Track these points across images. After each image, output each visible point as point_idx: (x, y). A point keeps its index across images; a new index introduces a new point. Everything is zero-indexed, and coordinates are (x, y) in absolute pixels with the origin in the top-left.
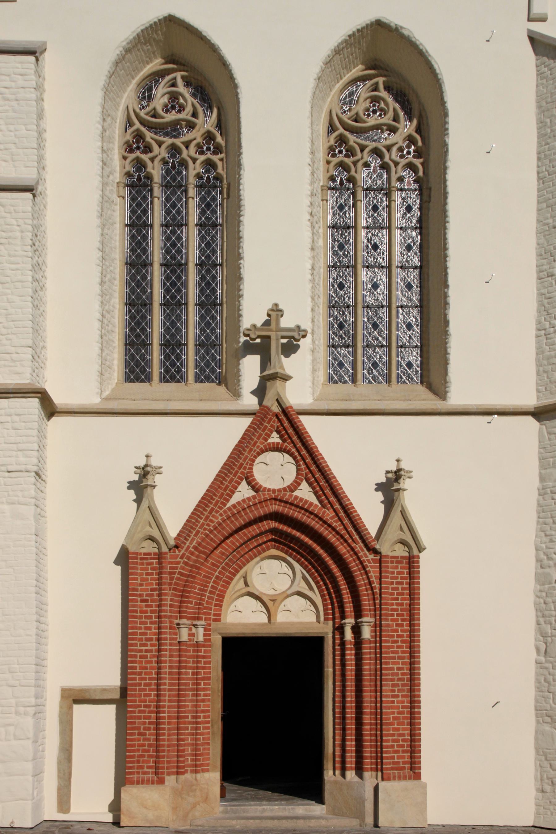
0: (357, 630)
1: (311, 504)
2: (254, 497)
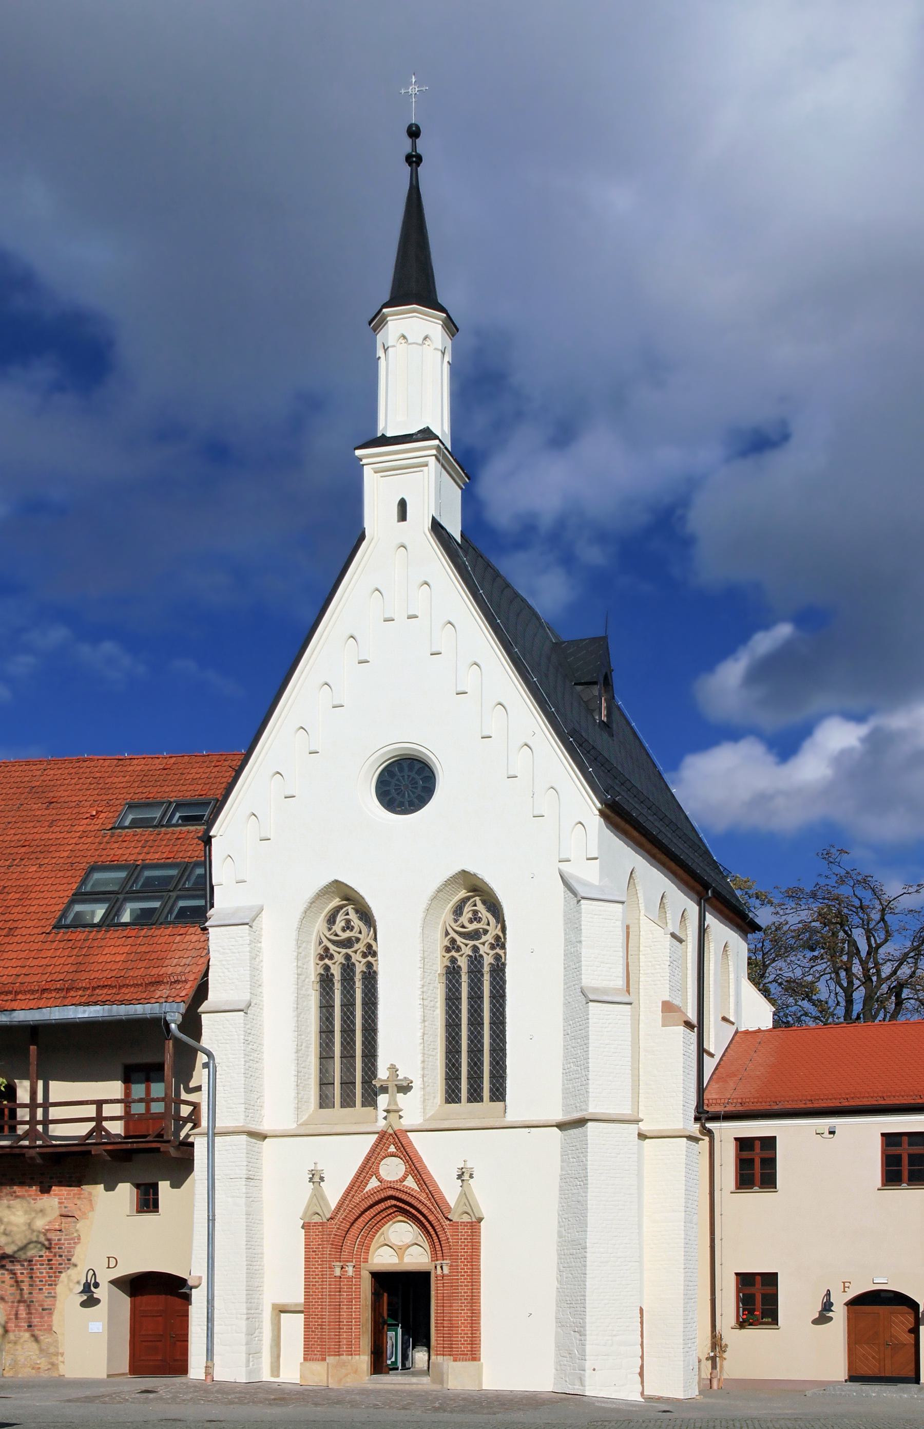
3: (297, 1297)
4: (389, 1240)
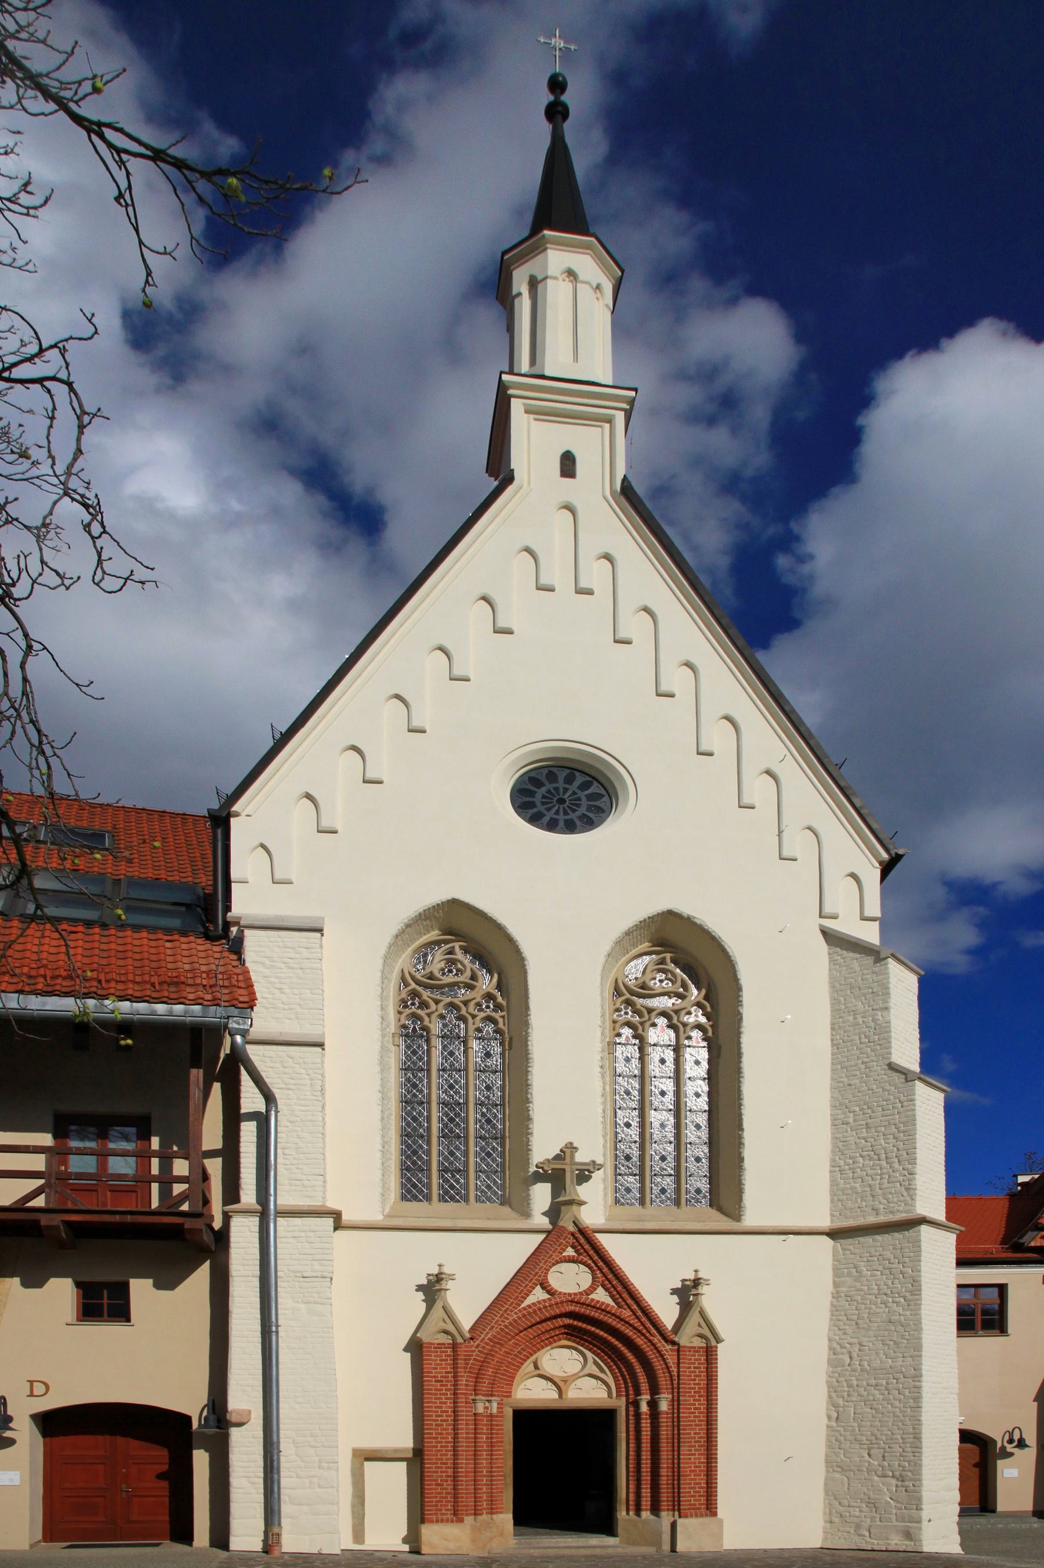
0: (653, 1404)
1: (608, 1305)
2: (549, 1299)
3: (406, 1441)
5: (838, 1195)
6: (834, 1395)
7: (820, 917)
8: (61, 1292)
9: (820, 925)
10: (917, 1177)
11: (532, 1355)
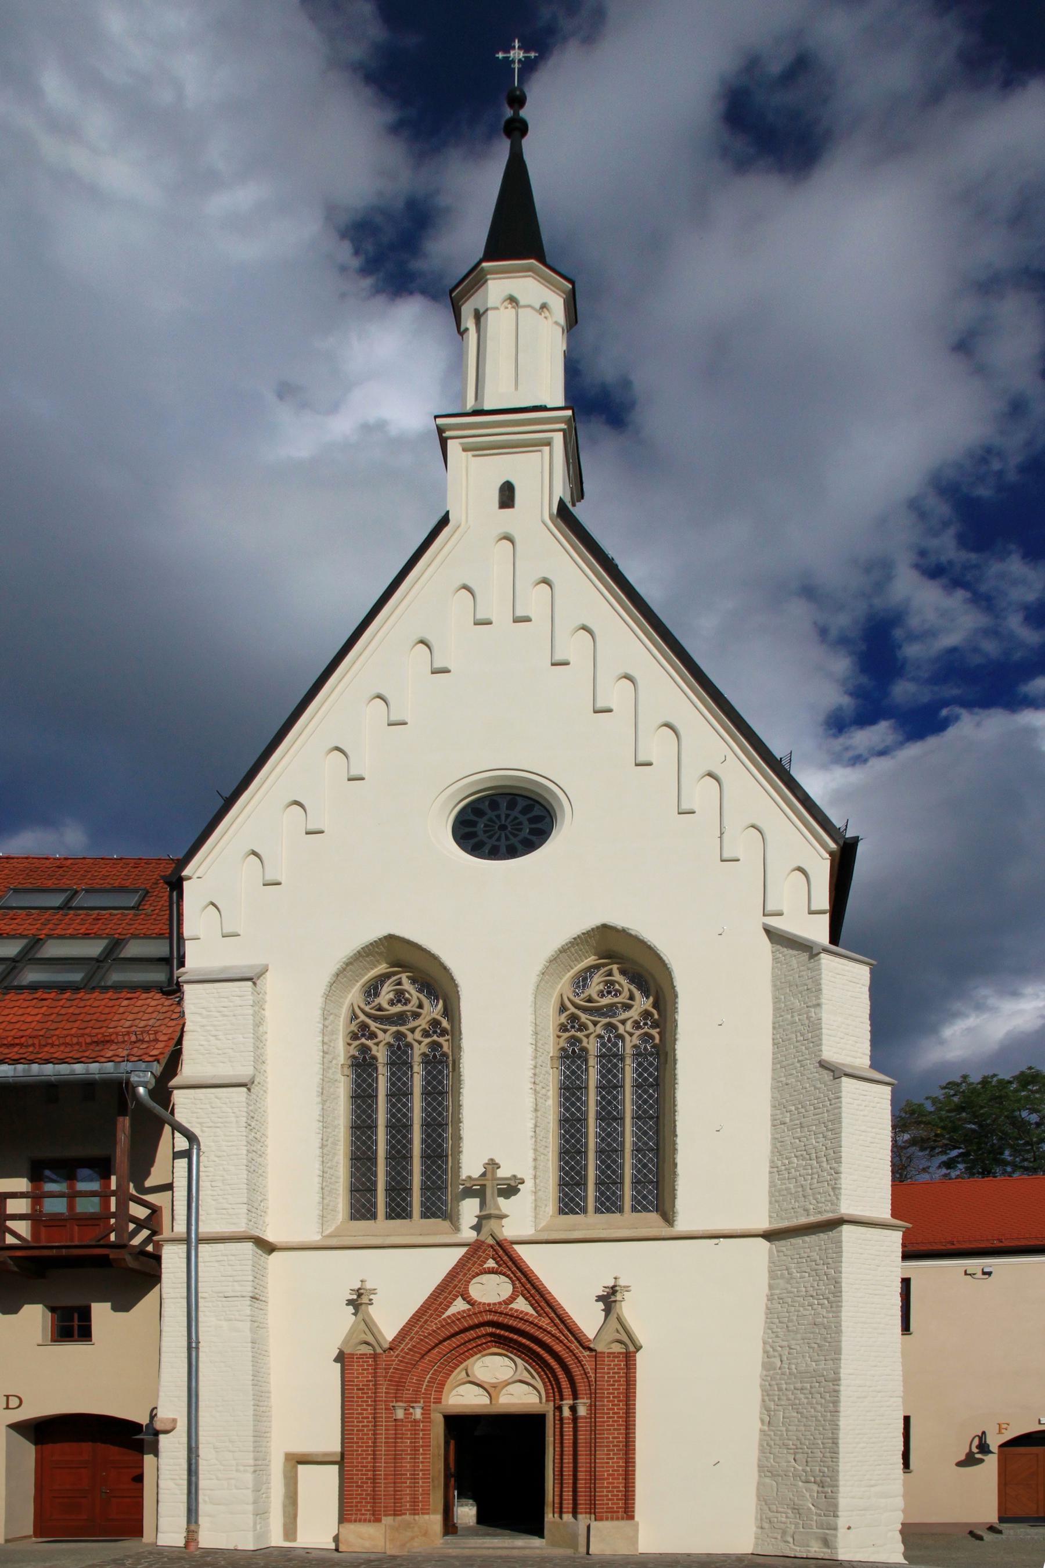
0: (573, 1409)
1: (527, 1314)
2: (469, 1310)
3: (333, 1444)
4: (475, 1376)
5: (776, 1195)
6: (766, 1398)
7: (764, 915)
8: (34, 1317)
9: (764, 924)
10: (842, 1176)
11: (462, 1363)
